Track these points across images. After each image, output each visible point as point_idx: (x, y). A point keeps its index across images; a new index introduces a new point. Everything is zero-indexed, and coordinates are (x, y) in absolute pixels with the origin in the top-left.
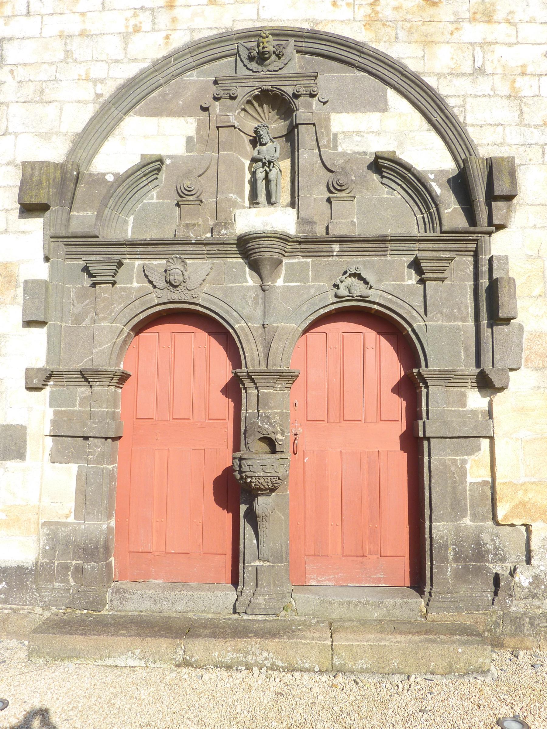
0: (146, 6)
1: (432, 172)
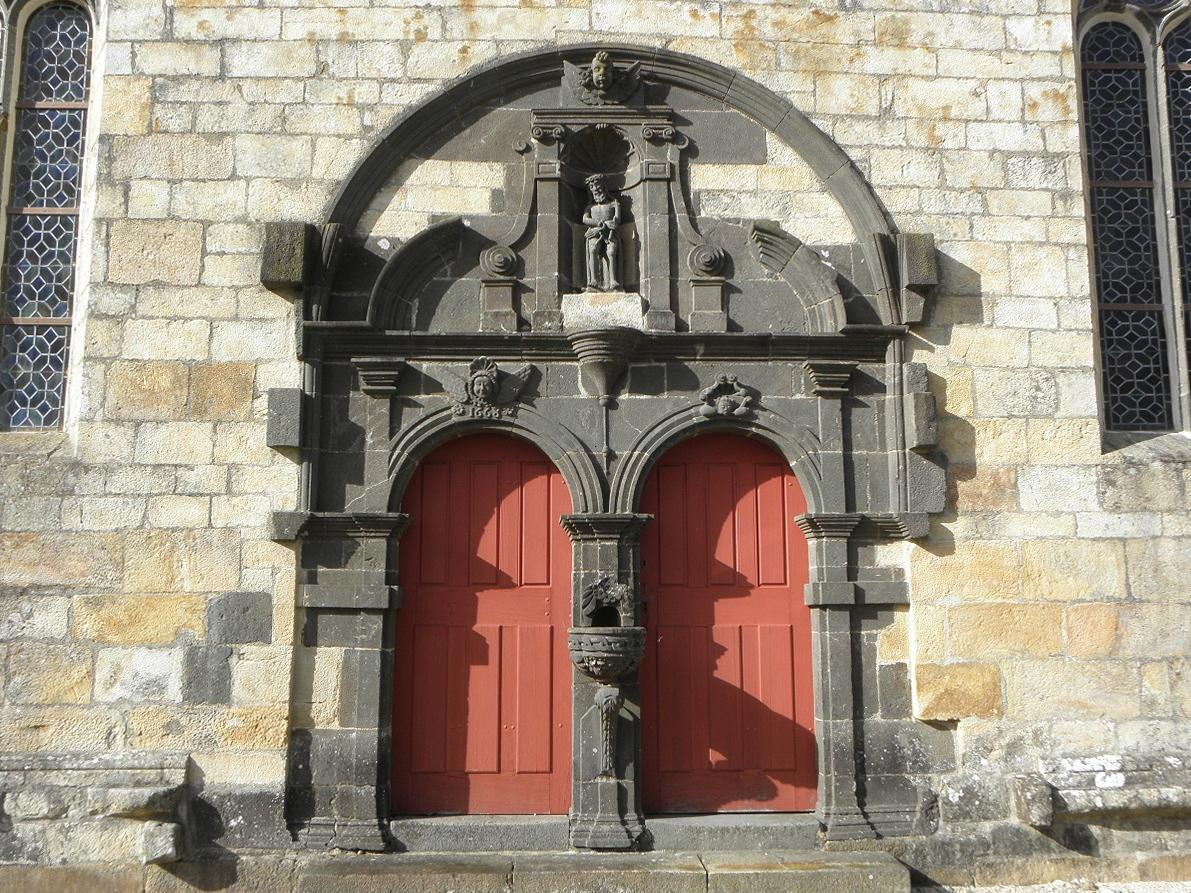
1: (826, 248)
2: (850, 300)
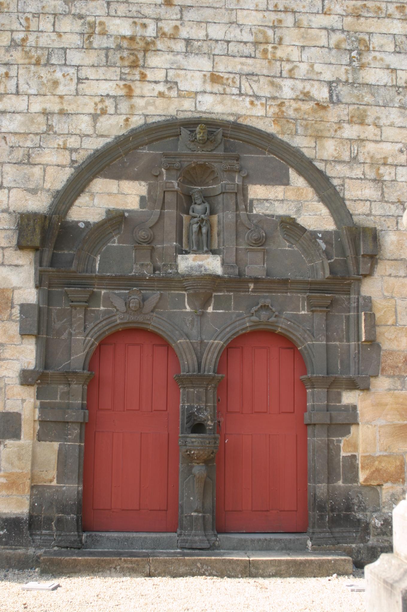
0: (111, 94)
1: (320, 232)
2: (332, 260)
